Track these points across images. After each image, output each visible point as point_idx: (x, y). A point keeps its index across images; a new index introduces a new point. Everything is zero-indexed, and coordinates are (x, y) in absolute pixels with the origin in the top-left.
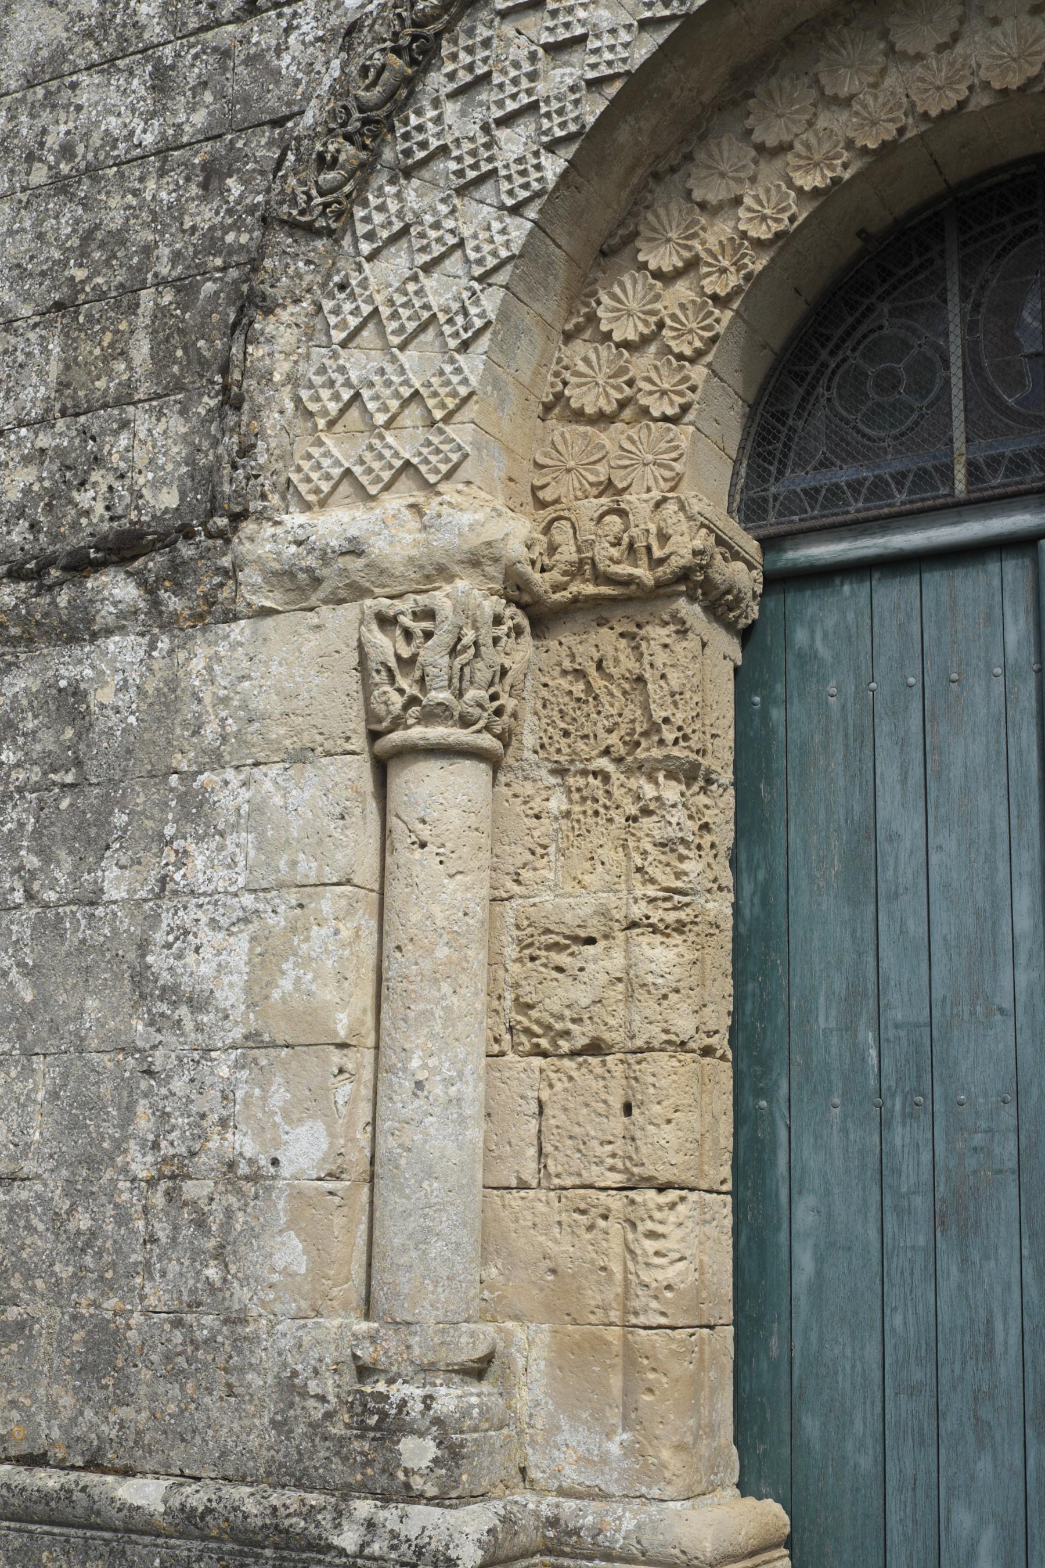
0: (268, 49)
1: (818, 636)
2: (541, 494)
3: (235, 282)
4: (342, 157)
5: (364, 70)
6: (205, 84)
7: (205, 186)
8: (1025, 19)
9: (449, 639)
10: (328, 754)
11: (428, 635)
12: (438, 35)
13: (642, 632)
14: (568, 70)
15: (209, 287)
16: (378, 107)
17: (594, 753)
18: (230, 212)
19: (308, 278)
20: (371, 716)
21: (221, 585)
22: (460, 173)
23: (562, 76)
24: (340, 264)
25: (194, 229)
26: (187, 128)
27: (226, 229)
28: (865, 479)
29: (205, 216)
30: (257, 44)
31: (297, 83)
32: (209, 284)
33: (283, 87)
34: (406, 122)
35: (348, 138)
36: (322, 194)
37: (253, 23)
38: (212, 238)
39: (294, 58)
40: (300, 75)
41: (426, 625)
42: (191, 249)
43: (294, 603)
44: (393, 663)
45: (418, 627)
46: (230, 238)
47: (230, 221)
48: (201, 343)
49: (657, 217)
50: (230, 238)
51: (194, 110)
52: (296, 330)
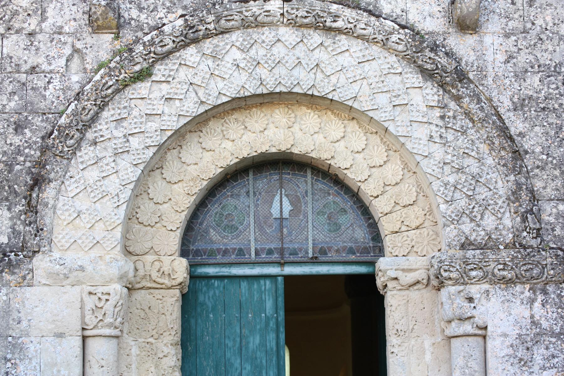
0: (41, 87)
1: (207, 297)
2: (128, 248)
3: (29, 167)
4: (76, 136)
5: (84, 109)
6: (15, 93)
7: (16, 130)
8: (286, 131)
9: (115, 303)
10: (71, 336)
11: (107, 300)
12: (109, 101)
13: (164, 299)
14: (154, 123)
15: (18, 167)
16: (88, 121)
17: (148, 336)
18: (26, 141)
19: (60, 173)
20: (83, 322)
21: (29, 273)
22: (115, 149)
23: (153, 125)
24: (70, 169)
25: (11, 144)
26: (7, 107)
27: (26, 148)
28: (222, 249)
29: (17, 140)
30: (36, 84)
31: (53, 102)
32: (18, 166)
33: (47, 102)
34: (96, 127)
35: (77, 130)
36: (68, 147)
37: (34, 76)
38: (19, 150)
39: (51, 93)
40: (54, 100)
41: (107, 297)
42: (10, 152)
43: (56, 283)
44: (94, 308)
45: (104, 297)
46: (27, 151)
47: (26, 145)
48: (16, 186)
49: (169, 164)
50: (27, 151)
51: (10, 101)
52: (55, 191)
